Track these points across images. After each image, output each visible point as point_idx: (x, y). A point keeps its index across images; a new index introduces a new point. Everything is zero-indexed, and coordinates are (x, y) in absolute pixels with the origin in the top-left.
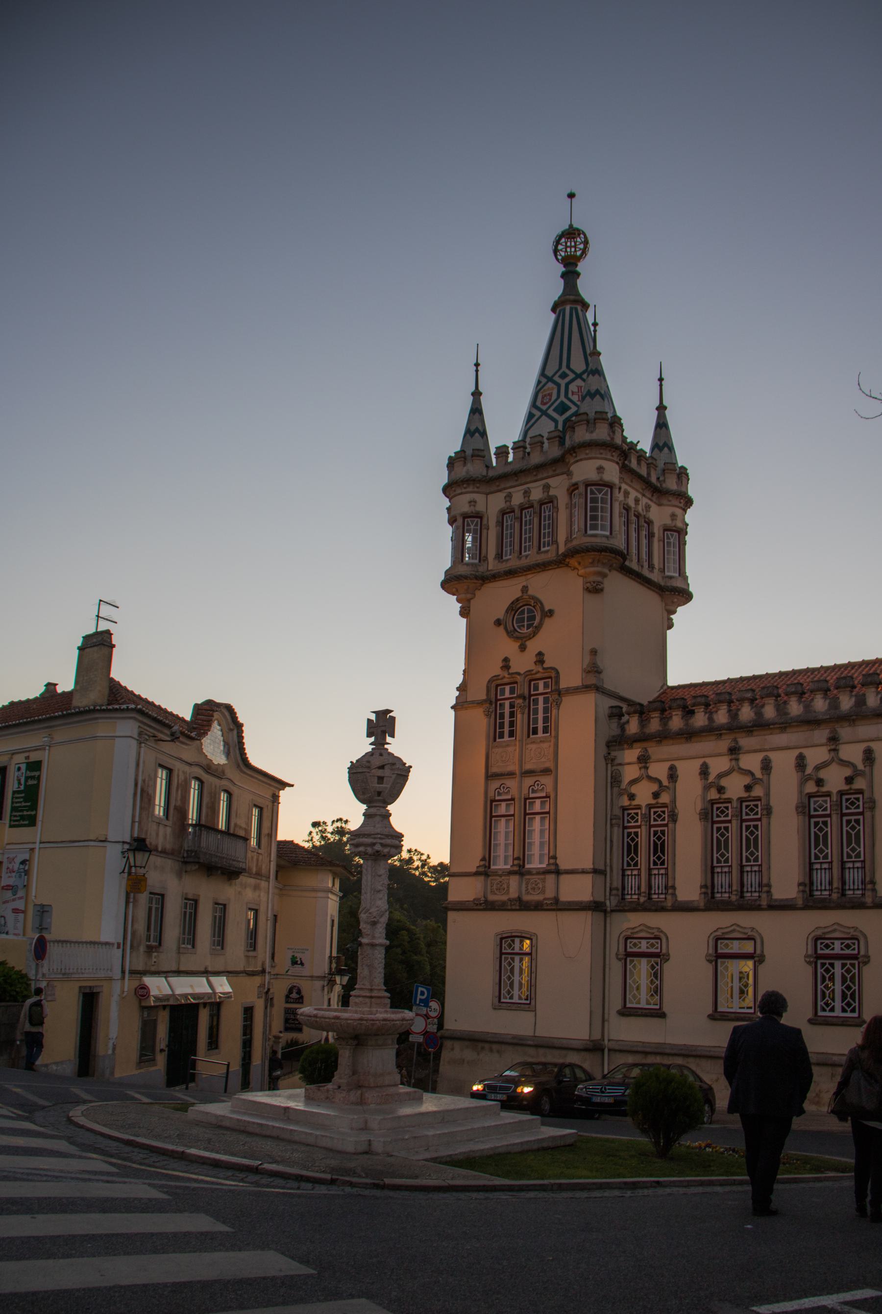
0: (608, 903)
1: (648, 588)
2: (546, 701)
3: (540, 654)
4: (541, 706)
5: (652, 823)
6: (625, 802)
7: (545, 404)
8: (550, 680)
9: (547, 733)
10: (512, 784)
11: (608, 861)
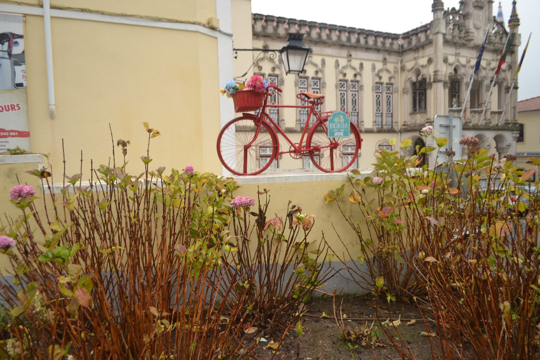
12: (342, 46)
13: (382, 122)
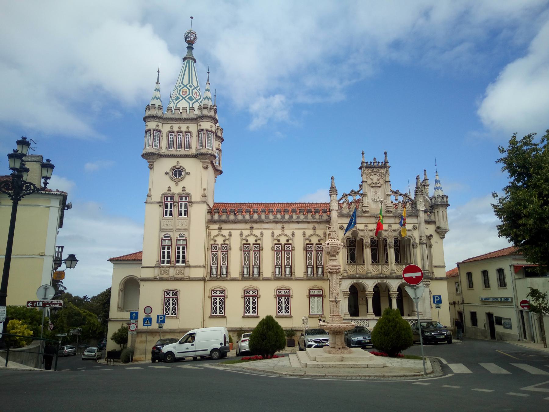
0: (206, 277)
1: (213, 169)
2: (186, 204)
3: (184, 187)
4: (183, 206)
5: (222, 250)
6: (212, 242)
7: (184, 95)
8: (187, 197)
9: (186, 216)
10: (170, 233)
11: (206, 263)
12: (277, 222)
13: (313, 272)
